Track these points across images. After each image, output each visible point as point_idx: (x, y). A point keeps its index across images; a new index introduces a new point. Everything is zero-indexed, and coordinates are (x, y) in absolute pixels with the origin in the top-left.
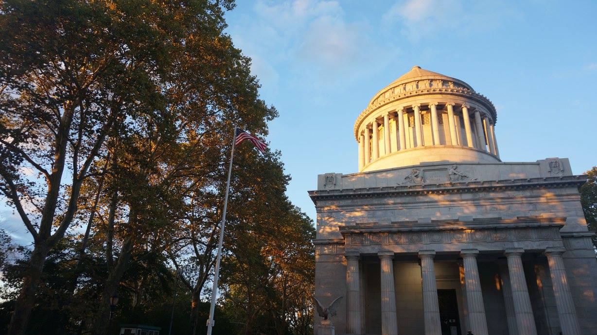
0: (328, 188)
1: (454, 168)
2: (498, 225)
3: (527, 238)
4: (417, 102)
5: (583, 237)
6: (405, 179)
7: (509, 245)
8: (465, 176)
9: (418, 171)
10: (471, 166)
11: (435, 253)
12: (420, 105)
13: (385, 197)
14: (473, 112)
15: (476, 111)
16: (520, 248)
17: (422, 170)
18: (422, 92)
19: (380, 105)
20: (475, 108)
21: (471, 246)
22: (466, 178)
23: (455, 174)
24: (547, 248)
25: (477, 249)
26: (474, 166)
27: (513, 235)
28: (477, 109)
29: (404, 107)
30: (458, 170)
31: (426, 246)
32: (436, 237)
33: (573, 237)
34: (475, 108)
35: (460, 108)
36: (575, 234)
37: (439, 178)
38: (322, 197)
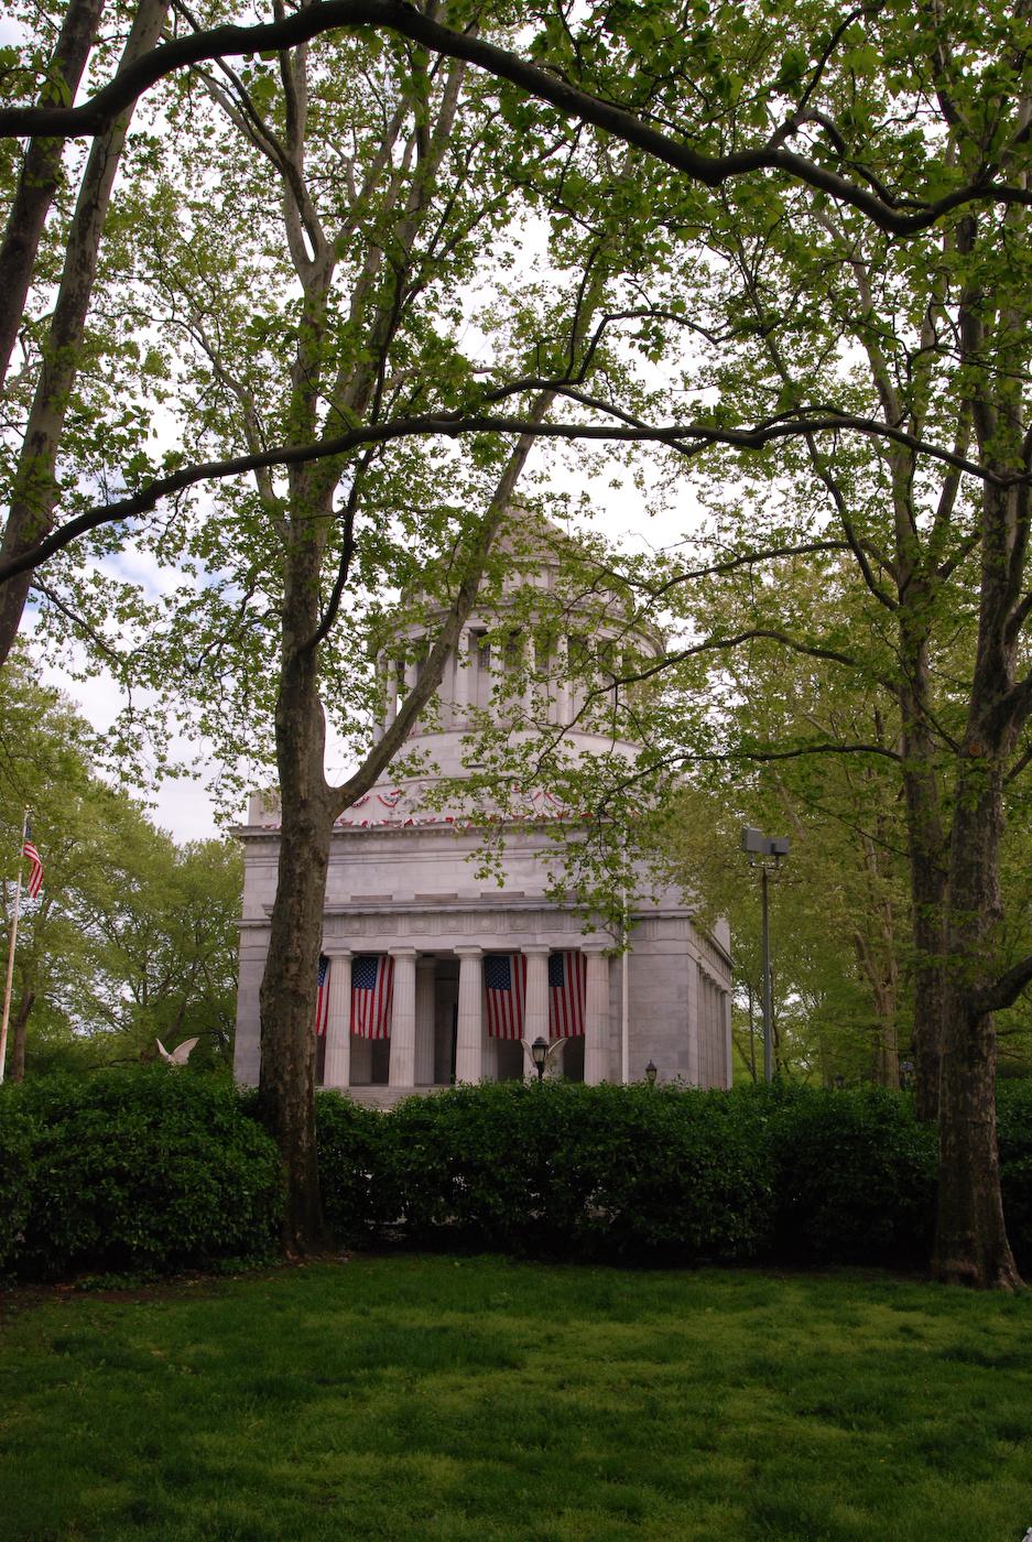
0: (264, 824)
2: (514, 907)
3: (559, 929)
5: (674, 918)
7: (529, 940)
11: (413, 952)
13: (366, 840)
16: (543, 945)
21: (471, 941)
24: (585, 944)
25: (478, 946)
27: (538, 924)
31: (404, 941)
32: (420, 924)
33: (658, 918)
36: (662, 914)
38: (255, 837)
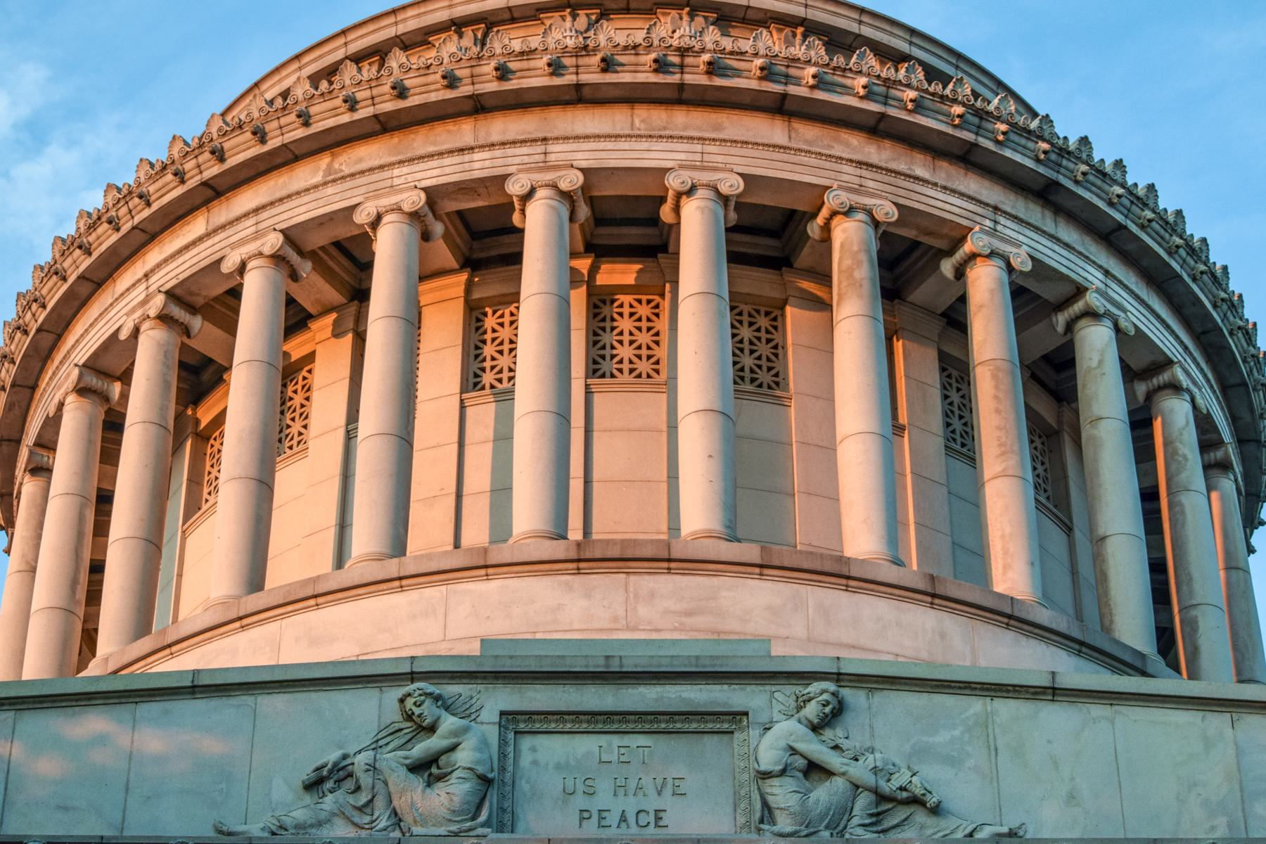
1: (812, 710)
4: (558, 152)
6: (314, 785)
8: (916, 801)
9: (449, 722)
10: (975, 706)
12: (571, 180)
14: (1061, 319)
15: (1092, 314)
17: (490, 714)
18: (608, 65)
19: (213, 170)
20: (1080, 291)
22: (920, 817)
23: (814, 770)
26: (1005, 709)
28: (1093, 299)
29: (433, 195)
30: (852, 732)
34: (1080, 291)
35: (947, 267)
37: (652, 803)
